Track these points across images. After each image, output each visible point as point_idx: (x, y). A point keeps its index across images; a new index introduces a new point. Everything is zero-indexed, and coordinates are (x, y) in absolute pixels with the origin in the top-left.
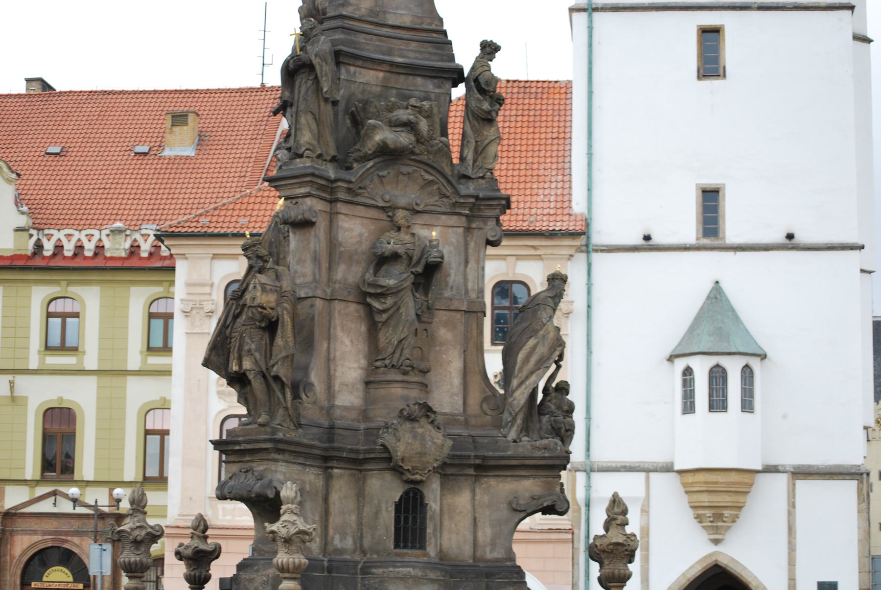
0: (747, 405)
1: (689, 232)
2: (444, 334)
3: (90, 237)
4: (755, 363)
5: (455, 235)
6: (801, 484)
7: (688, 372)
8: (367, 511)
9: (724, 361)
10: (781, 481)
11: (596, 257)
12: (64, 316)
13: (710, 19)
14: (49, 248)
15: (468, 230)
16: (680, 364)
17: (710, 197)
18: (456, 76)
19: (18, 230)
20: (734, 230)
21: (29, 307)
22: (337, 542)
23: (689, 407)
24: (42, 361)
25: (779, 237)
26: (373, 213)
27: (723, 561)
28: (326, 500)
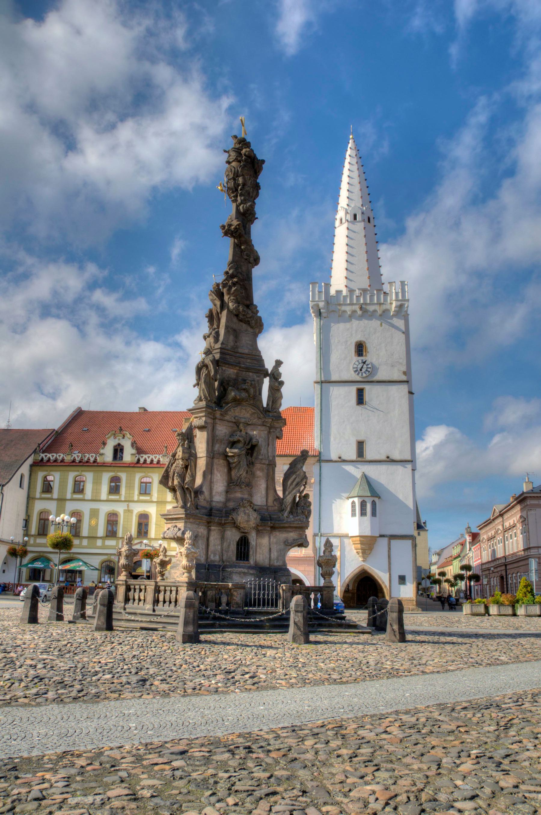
0: (374, 514)
1: (354, 457)
2: (259, 473)
3: (156, 457)
4: (376, 499)
5: (264, 434)
6: (393, 542)
7: (353, 503)
8: (225, 544)
9: (366, 499)
10: (386, 540)
11: (323, 464)
12: (146, 483)
13: (361, 386)
14: (142, 460)
15: (269, 432)
16: (351, 500)
17: (361, 445)
18: (266, 374)
19: (132, 454)
20: (369, 454)
21: (134, 480)
22: (212, 557)
23: (353, 515)
24: (139, 498)
25: (384, 458)
26: (231, 424)
27: (366, 568)
28: (208, 539)
